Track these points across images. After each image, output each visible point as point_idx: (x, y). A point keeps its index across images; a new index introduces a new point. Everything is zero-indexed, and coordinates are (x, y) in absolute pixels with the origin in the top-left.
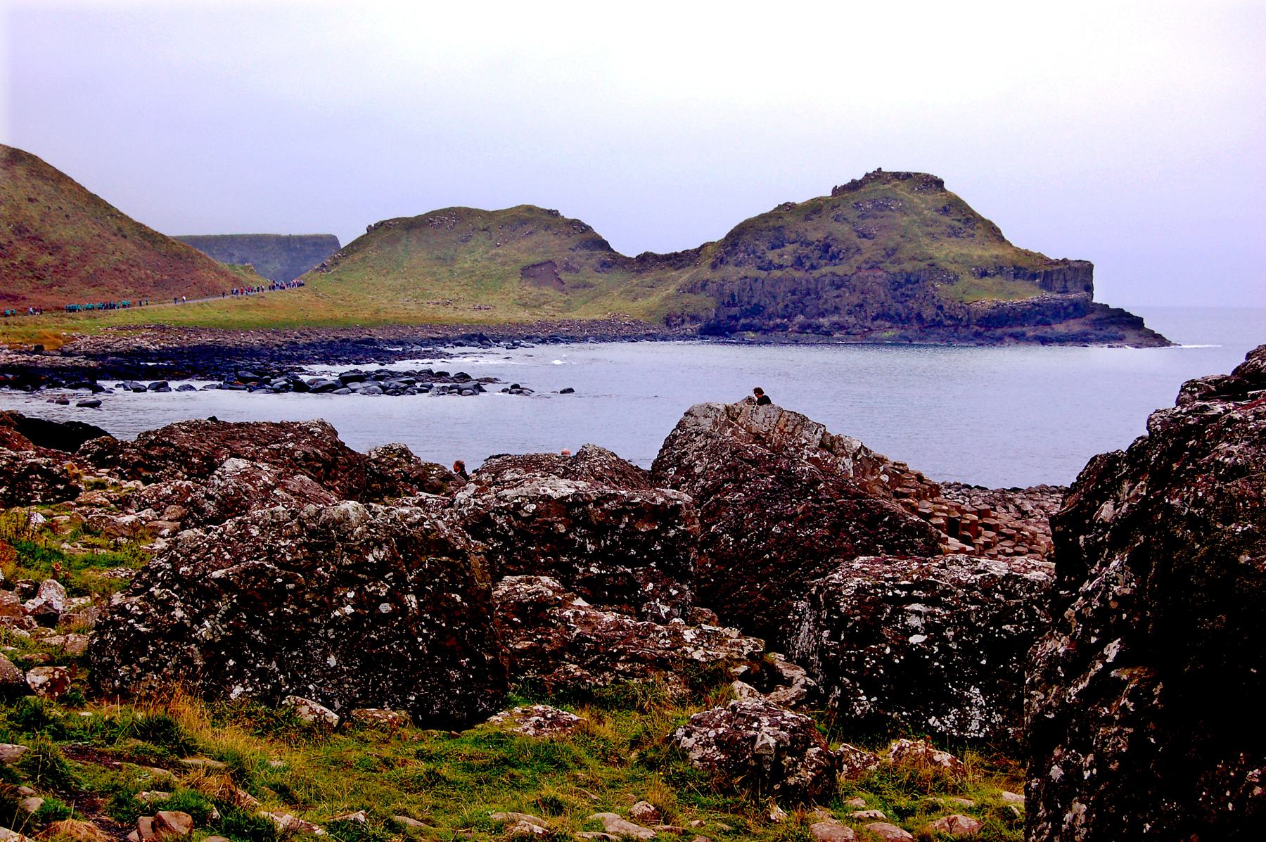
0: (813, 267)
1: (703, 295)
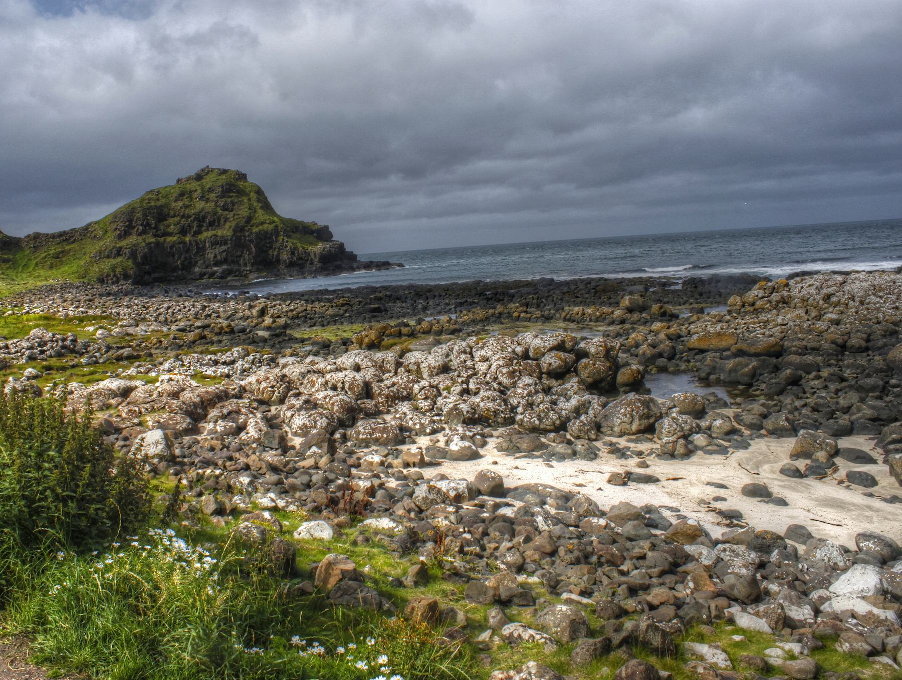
0: (198, 232)
1: (120, 259)
